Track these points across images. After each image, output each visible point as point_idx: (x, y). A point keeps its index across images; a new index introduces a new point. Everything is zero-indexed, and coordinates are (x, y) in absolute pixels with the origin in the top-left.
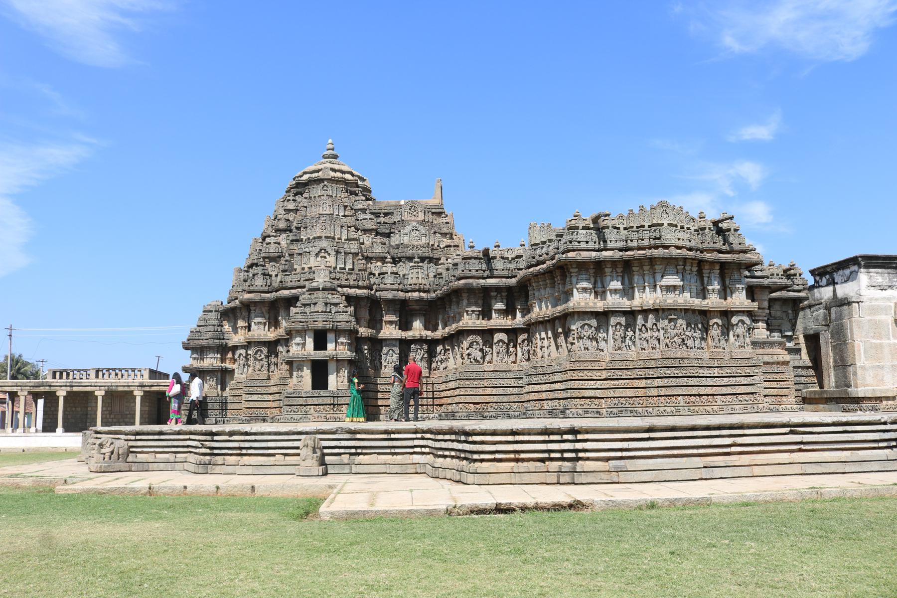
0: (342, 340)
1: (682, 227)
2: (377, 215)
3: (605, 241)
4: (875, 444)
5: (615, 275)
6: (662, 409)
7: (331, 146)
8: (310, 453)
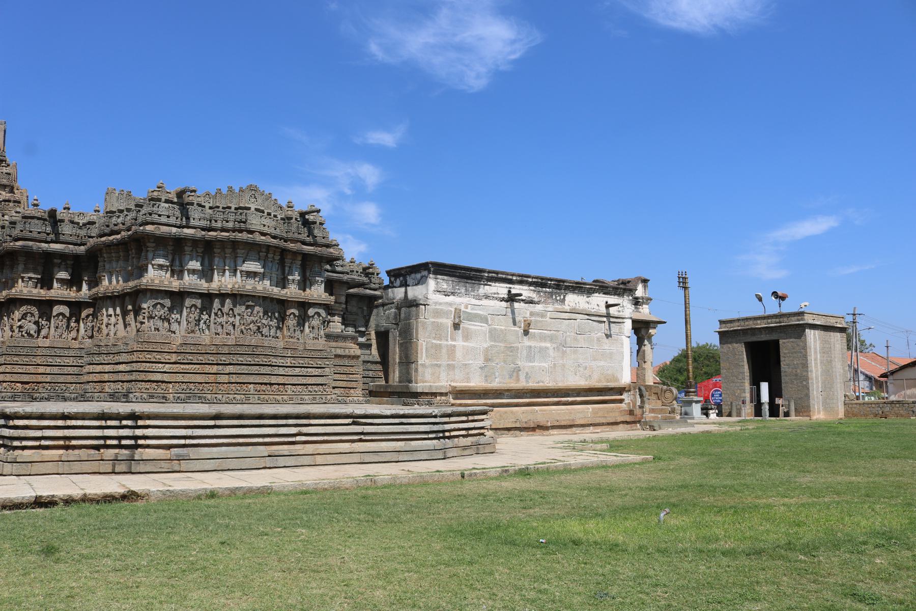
1: (269, 214)
3: (188, 218)
5: (194, 254)
6: (231, 396)
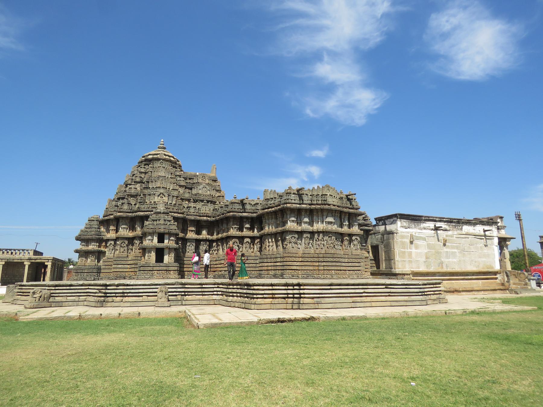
0: (172, 238)
2: (186, 179)
3: (303, 200)
4: (417, 294)
7: (162, 143)
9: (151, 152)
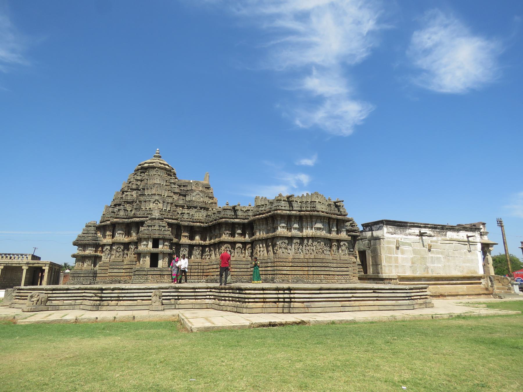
0: (166, 243)
2: (180, 186)
3: (292, 207)
4: (404, 298)
7: (158, 152)
8: (158, 299)
9: (147, 161)
